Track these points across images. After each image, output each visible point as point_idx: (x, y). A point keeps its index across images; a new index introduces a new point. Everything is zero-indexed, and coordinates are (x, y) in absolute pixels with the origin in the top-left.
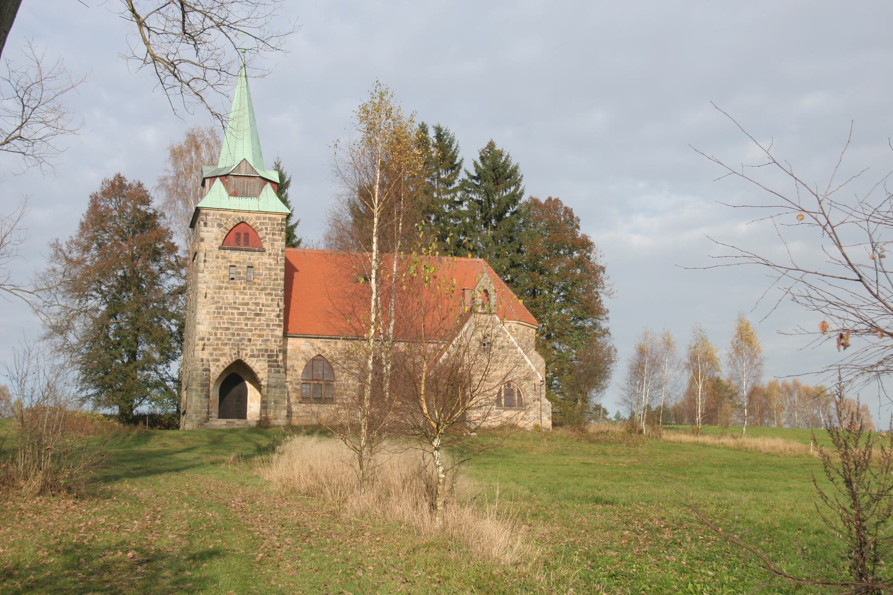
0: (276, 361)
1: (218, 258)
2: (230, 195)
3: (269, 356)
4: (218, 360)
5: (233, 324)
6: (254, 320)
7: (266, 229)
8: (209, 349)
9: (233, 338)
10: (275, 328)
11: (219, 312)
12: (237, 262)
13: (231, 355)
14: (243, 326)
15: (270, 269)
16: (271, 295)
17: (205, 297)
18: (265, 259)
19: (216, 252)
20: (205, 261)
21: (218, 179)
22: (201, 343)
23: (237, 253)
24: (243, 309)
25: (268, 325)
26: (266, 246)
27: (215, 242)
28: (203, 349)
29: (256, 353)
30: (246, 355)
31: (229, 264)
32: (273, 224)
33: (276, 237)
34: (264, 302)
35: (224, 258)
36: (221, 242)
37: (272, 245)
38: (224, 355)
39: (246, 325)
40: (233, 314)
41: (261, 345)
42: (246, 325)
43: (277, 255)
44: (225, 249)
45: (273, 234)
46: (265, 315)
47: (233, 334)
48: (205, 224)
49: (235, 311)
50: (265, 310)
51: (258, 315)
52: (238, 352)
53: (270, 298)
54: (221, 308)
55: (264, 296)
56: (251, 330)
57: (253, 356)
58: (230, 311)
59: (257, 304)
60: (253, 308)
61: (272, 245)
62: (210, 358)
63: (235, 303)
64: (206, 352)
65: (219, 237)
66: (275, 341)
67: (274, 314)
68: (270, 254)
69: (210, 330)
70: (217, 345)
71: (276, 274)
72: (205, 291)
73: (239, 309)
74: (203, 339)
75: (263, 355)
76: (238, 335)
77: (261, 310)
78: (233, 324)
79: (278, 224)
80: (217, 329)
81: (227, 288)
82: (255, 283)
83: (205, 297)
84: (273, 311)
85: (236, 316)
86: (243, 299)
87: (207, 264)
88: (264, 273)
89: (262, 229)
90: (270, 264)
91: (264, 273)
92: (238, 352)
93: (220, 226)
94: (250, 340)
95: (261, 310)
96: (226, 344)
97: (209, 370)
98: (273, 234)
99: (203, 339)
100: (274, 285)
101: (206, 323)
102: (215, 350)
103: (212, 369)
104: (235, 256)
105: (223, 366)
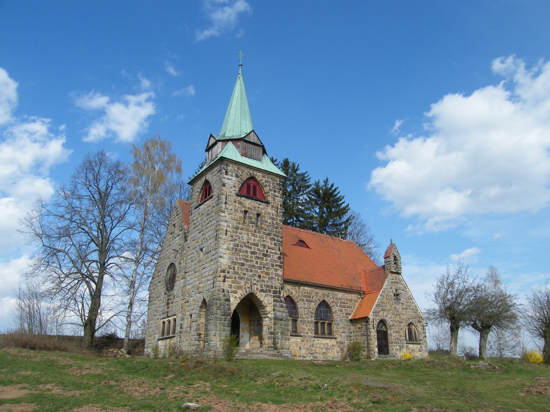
0: (279, 297)
1: (235, 202)
2: (242, 155)
3: (275, 292)
4: (236, 292)
5: (247, 261)
6: (262, 259)
7: (270, 186)
8: (229, 282)
9: (247, 273)
10: (278, 268)
11: (236, 249)
12: (249, 208)
13: (245, 289)
14: (254, 263)
15: (273, 219)
16: (274, 240)
17: (226, 234)
18: (269, 210)
19: (234, 197)
20: (226, 203)
21: (230, 144)
22: (222, 274)
23: (250, 201)
24: (254, 248)
25: (273, 265)
26: (270, 199)
27: (234, 189)
28: (224, 281)
29: (264, 288)
30: (257, 289)
31: (243, 209)
32: (274, 183)
33: (277, 194)
34: (270, 246)
35: (240, 203)
36: (237, 189)
37: (274, 199)
38: (240, 288)
39: (257, 263)
40: (247, 252)
41: (268, 281)
42: (257, 263)
43: (277, 208)
44: (241, 196)
45: (275, 191)
46: (270, 256)
47: (247, 270)
48: (227, 173)
49: (249, 250)
50: (271, 253)
51: (265, 255)
52: (251, 286)
53: (274, 242)
54: (238, 246)
55: (269, 240)
56: (260, 268)
57: (262, 291)
58: (244, 248)
59: (264, 246)
60: (261, 249)
61: (274, 199)
62: (230, 289)
63: (248, 242)
64: (226, 284)
65: (237, 185)
66: (278, 280)
67: (276, 256)
68: (272, 207)
69: (230, 264)
70: (235, 278)
71: (277, 223)
72: (225, 229)
73: (251, 248)
74: (223, 271)
75: (270, 291)
76: (251, 271)
77: (267, 251)
78: (247, 261)
79: (277, 184)
80: (235, 263)
81: (242, 229)
82: (262, 228)
83: (226, 234)
84: (276, 254)
85: (250, 255)
86: (254, 240)
87: (227, 206)
88: (269, 221)
89: (266, 186)
90: (273, 215)
91: (269, 221)
92: (251, 286)
93: (237, 176)
94: (259, 276)
95: (267, 251)
96: (242, 278)
97: (230, 301)
98: (275, 191)
99: (223, 271)
100: (276, 232)
101: (226, 257)
102: (234, 282)
103: (232, 299)
104: (248, 203)
105: (240, 298)
